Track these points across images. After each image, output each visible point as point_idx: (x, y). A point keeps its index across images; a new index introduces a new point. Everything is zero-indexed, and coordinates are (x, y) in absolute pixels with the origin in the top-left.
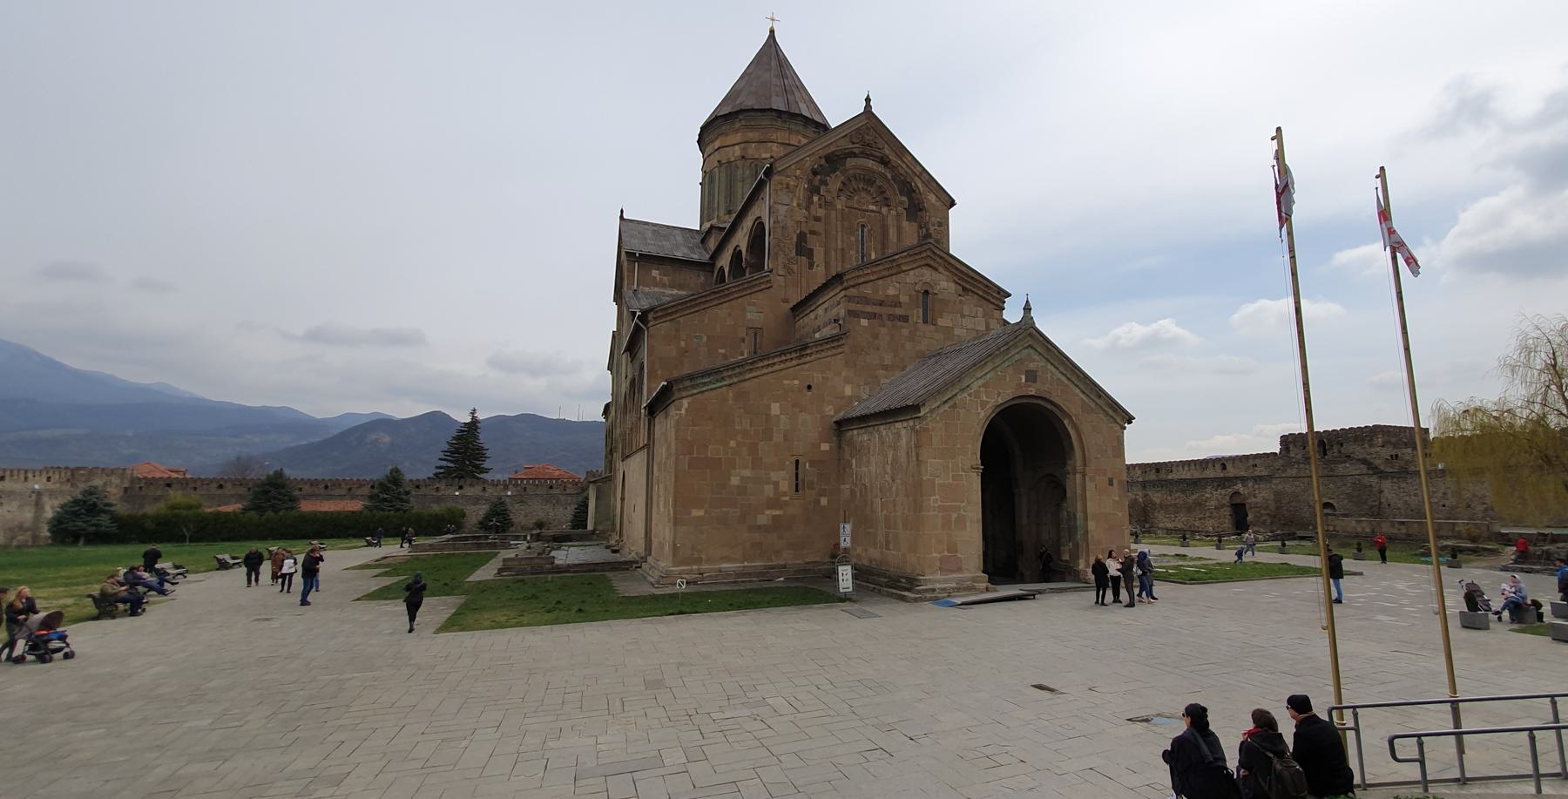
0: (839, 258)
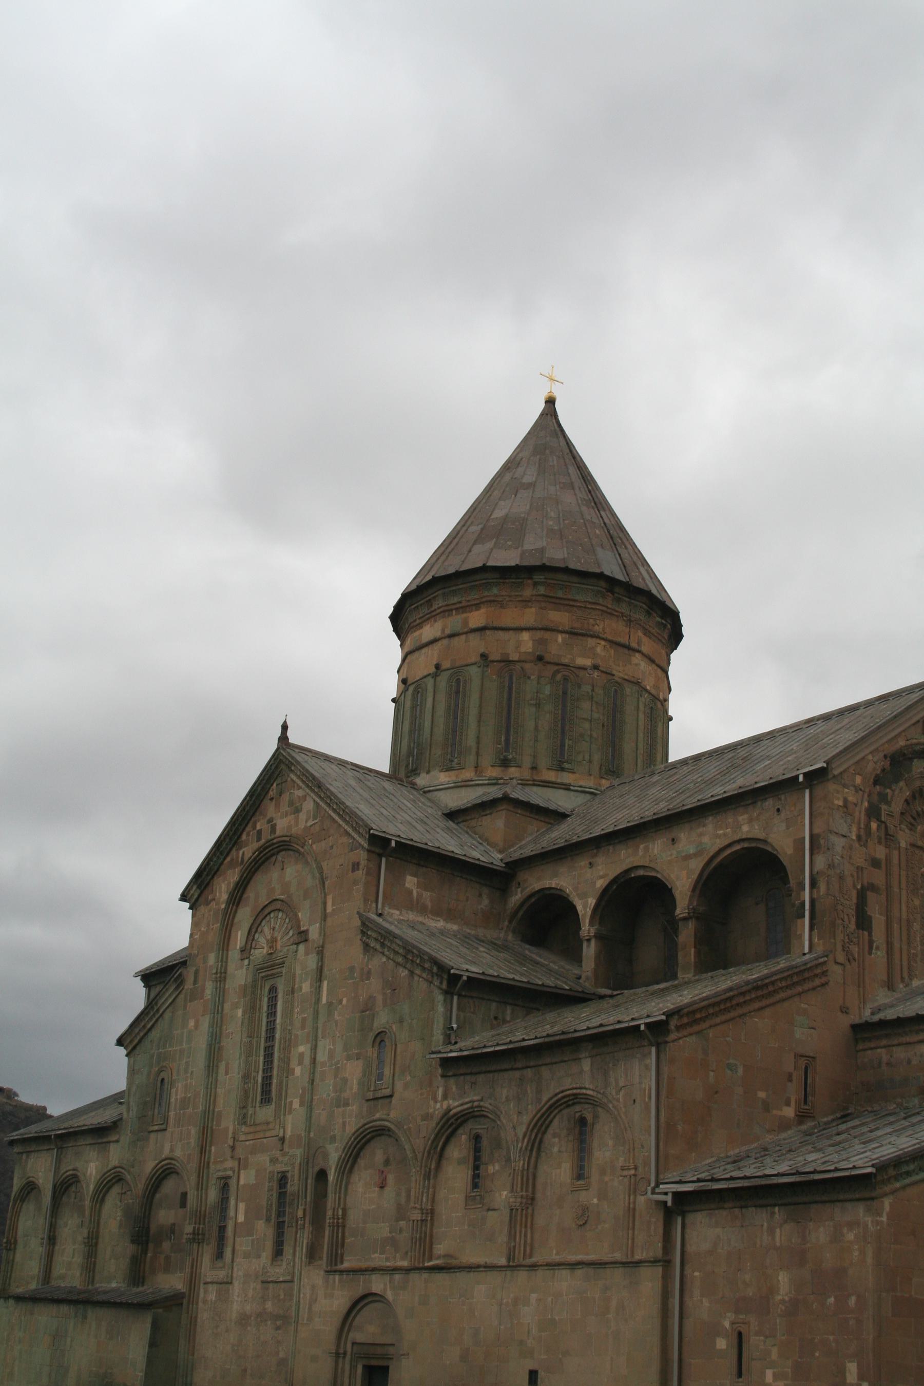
0: (904, 938)
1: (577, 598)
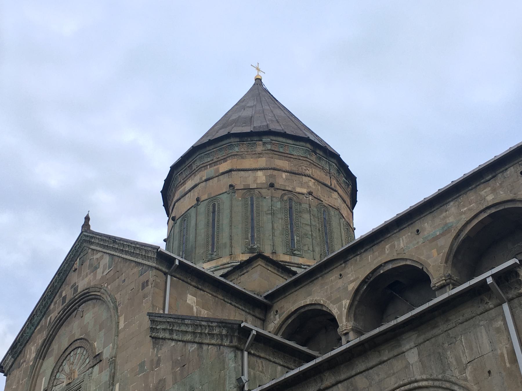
1: (293, 153)
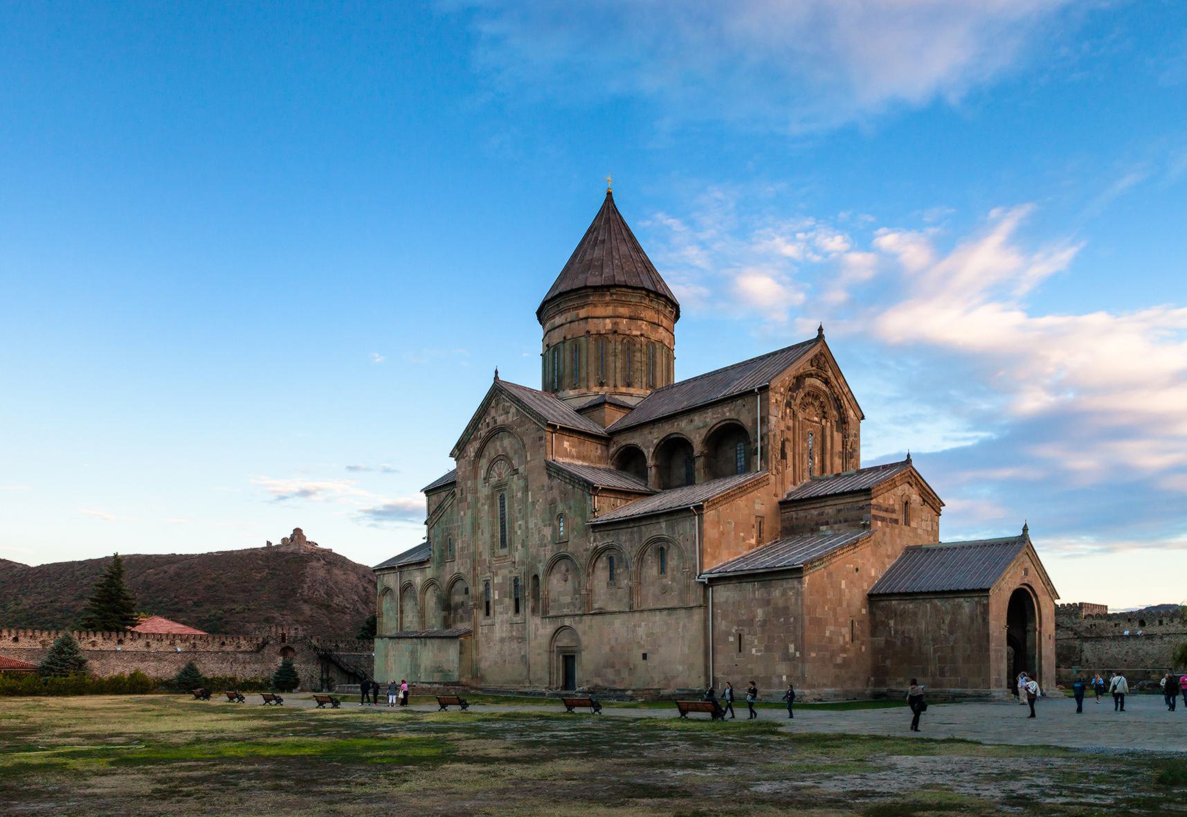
1: (632, 300)
